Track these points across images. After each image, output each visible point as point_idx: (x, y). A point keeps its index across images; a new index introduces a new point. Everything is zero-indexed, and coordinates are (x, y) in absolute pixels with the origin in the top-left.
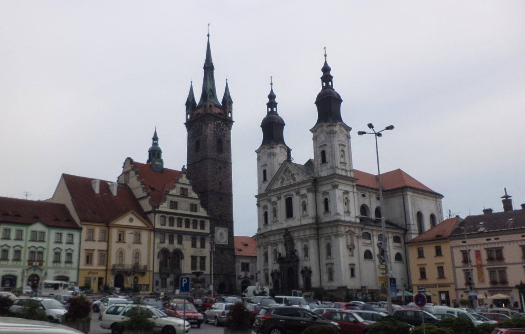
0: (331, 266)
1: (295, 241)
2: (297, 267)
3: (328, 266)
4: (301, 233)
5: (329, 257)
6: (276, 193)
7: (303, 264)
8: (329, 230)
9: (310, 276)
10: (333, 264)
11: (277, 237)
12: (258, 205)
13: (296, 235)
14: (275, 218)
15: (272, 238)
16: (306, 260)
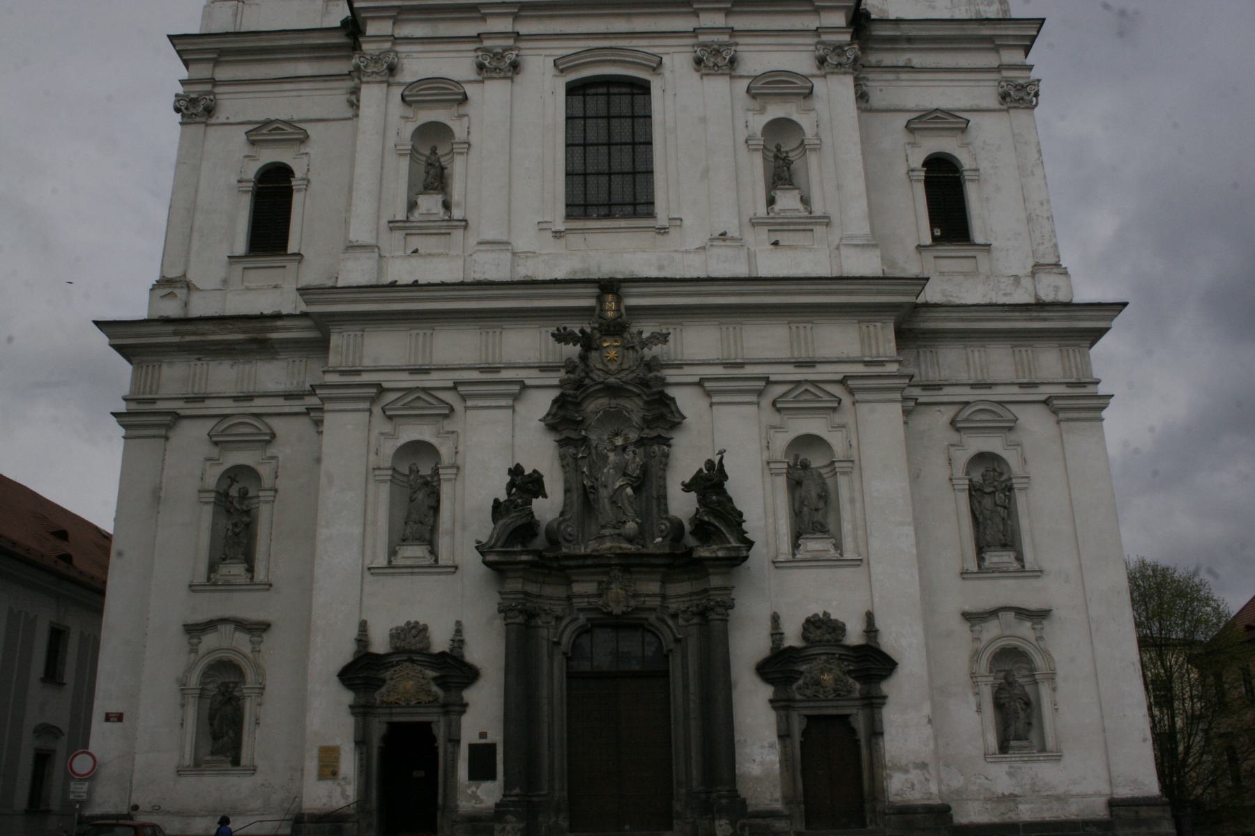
0: (1025, 629)
1: (686, 400)
2: (712, 619)
3: (992, 630)
4: (766, 341)
5: (1002, 558)
6: (470, 29)
7: (778, 597)
8: (999, 362)
9: (874, 702)
10: (1039, 616)
11: (456, 347)
12: (195, 109)
13: (697, 343)
14: (430, 204)
15: (384, 350)
16: (816, 561)
